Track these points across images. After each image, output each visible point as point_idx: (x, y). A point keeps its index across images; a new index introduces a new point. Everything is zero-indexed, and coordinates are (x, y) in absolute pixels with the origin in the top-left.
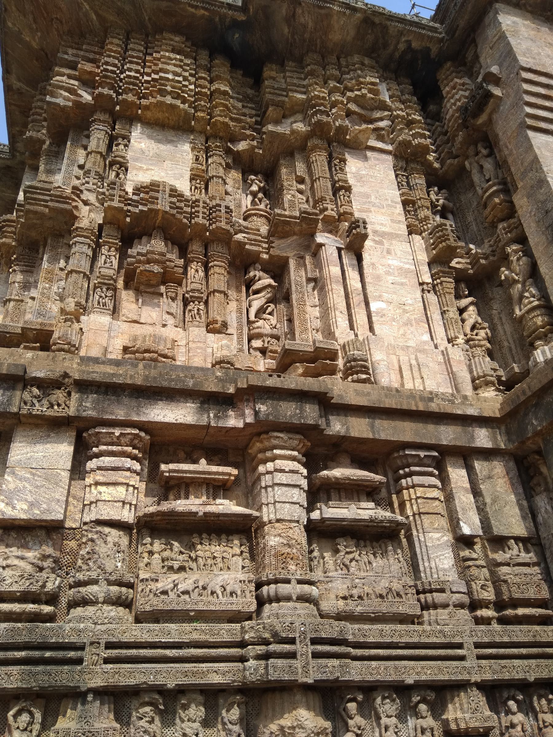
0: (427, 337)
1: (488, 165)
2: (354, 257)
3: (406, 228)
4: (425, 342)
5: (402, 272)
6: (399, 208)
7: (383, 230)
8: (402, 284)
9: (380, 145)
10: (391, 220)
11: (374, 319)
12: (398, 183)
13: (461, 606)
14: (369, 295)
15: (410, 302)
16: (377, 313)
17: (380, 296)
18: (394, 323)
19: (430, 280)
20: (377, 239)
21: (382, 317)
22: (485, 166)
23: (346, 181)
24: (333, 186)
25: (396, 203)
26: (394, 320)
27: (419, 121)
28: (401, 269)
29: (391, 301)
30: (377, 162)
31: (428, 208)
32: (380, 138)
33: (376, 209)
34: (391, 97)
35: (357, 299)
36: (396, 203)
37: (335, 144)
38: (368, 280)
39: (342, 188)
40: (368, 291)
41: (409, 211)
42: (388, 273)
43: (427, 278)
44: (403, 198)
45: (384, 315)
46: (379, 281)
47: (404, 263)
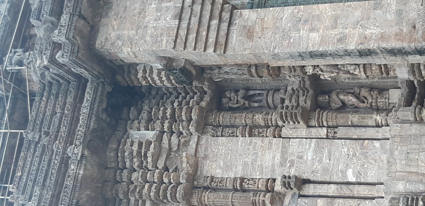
0: (377, 144)
2: (307, 185)
3: (276, 139)
4: (382, 146)
5: (318, 150)
6: (257, 141)
7: (279, 158)
8: (330, 153)
10: (268, 149)
11: (362, 181)
12: (230, 136)
15: (346, 150)
16: (357, 177)
17: (342, 172)
18: (366, 166)
19: (325, 130)
20: (289, 165)
21: (360, 174)
24: (236, 190)
25: (251, 142)
26: (362, 166)
28: (315, 151)
29: (345, 165)
30: (210, 150)
31: (254, 116)
32: (187, 143)
33: (258, 160)
35: (345, 191)
36: (251, 142)
37: (196, 183)
38: (328, 180)
40: (338, 181)
41: (259, 133)
42: (320, 161)
43: (323, 132)
44: (247, 135)
45: (359, 172)
46: (328, 170)
47: (310, 146)
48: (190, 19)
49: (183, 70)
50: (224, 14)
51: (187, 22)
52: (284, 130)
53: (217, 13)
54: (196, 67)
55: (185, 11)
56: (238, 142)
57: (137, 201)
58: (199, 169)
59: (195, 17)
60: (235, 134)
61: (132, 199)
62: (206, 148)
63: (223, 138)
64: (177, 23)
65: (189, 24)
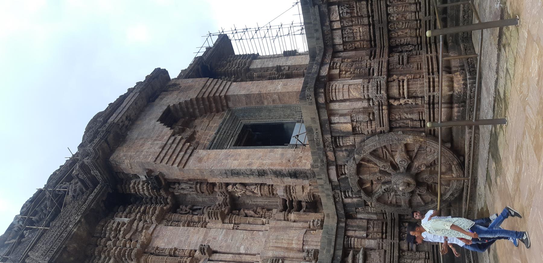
1: (183, 186)
6: (191, 229)
9: (151, 229)
12: (175, 226)
13: (383, 241)
14: (236, 252)
22: (183, 187)
23: (171, 249)
25: (187, 229)
27: (146, 208)
30: (161, 233)
34: (126, 217)
36: (187, 229)
39: (174, 253)
41: (193, 225)
44: (186, 226)
48: (168, 150)
49: (157, 178)
50: (188, 151)
51: (166, 151)
52: (208, 224)
53: (184, 149)
54: (165, 180)
55: (167, 146)
56: (180, 229)
57: (105, 258)
58: (151, 243)
59: (172, 149)
60: (179, 225)
61: (103, 256)
62: (159, 232)
63: (171, 227)
64: (161, 150)
65: (167, 152)
